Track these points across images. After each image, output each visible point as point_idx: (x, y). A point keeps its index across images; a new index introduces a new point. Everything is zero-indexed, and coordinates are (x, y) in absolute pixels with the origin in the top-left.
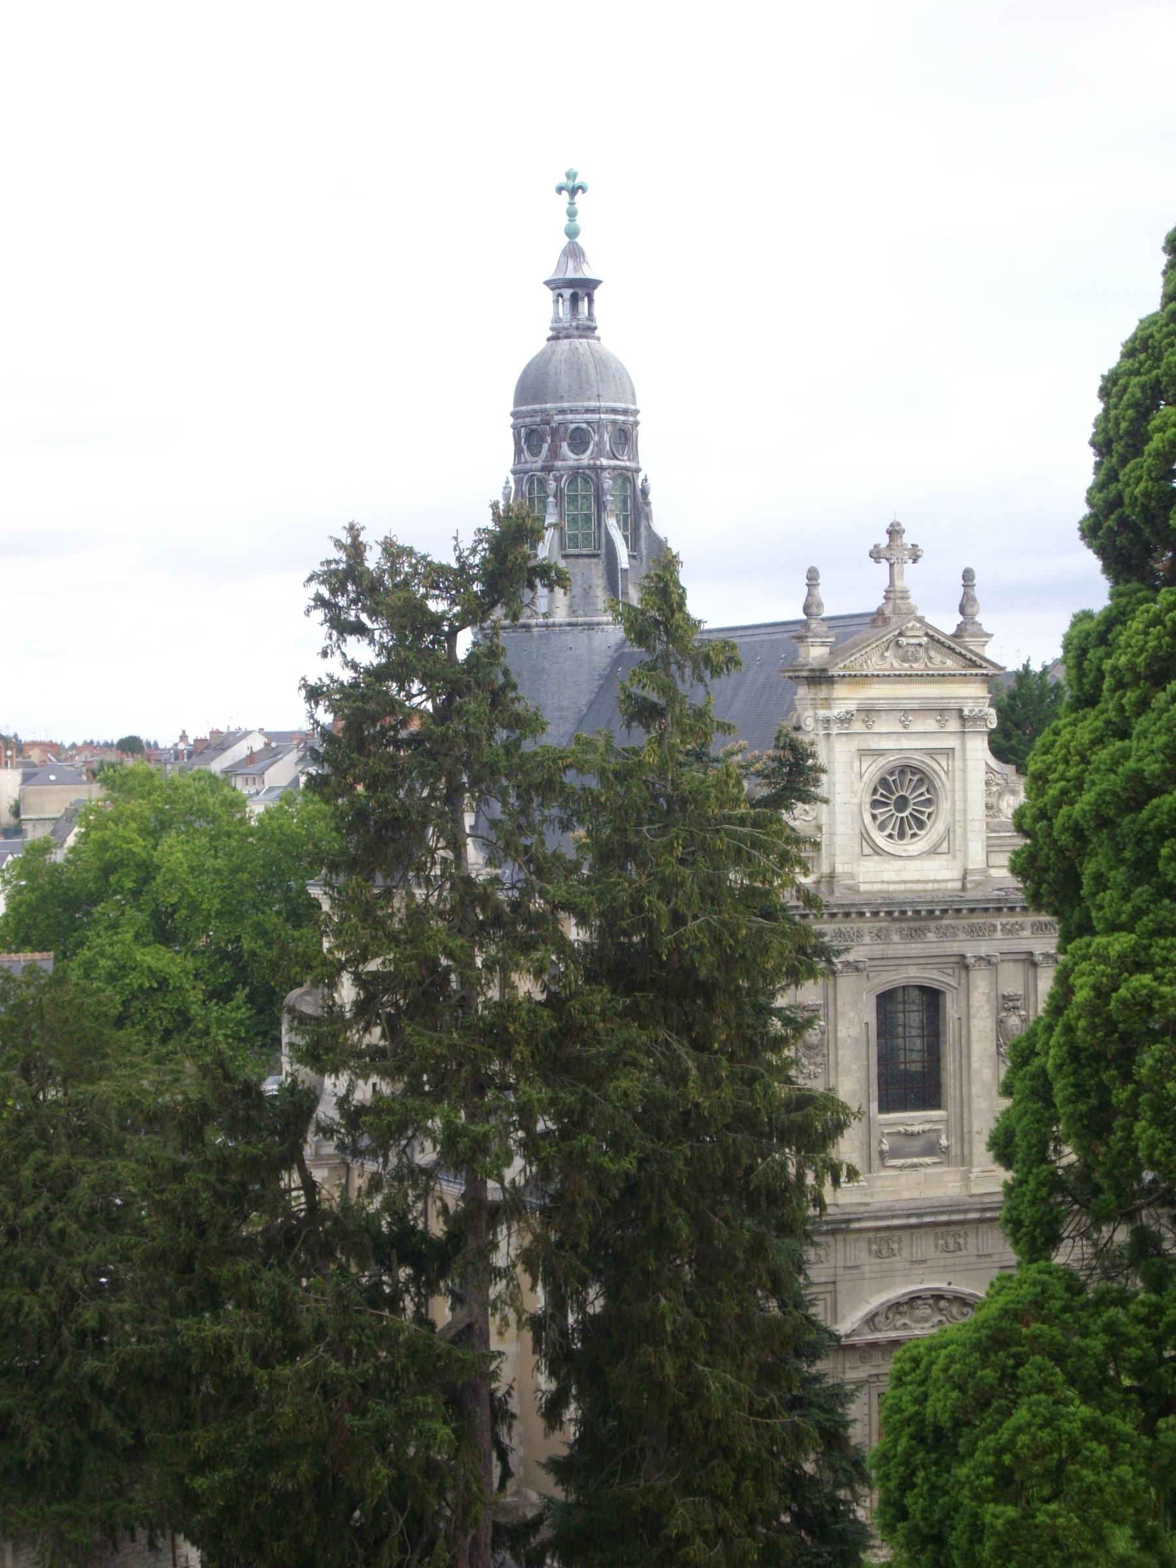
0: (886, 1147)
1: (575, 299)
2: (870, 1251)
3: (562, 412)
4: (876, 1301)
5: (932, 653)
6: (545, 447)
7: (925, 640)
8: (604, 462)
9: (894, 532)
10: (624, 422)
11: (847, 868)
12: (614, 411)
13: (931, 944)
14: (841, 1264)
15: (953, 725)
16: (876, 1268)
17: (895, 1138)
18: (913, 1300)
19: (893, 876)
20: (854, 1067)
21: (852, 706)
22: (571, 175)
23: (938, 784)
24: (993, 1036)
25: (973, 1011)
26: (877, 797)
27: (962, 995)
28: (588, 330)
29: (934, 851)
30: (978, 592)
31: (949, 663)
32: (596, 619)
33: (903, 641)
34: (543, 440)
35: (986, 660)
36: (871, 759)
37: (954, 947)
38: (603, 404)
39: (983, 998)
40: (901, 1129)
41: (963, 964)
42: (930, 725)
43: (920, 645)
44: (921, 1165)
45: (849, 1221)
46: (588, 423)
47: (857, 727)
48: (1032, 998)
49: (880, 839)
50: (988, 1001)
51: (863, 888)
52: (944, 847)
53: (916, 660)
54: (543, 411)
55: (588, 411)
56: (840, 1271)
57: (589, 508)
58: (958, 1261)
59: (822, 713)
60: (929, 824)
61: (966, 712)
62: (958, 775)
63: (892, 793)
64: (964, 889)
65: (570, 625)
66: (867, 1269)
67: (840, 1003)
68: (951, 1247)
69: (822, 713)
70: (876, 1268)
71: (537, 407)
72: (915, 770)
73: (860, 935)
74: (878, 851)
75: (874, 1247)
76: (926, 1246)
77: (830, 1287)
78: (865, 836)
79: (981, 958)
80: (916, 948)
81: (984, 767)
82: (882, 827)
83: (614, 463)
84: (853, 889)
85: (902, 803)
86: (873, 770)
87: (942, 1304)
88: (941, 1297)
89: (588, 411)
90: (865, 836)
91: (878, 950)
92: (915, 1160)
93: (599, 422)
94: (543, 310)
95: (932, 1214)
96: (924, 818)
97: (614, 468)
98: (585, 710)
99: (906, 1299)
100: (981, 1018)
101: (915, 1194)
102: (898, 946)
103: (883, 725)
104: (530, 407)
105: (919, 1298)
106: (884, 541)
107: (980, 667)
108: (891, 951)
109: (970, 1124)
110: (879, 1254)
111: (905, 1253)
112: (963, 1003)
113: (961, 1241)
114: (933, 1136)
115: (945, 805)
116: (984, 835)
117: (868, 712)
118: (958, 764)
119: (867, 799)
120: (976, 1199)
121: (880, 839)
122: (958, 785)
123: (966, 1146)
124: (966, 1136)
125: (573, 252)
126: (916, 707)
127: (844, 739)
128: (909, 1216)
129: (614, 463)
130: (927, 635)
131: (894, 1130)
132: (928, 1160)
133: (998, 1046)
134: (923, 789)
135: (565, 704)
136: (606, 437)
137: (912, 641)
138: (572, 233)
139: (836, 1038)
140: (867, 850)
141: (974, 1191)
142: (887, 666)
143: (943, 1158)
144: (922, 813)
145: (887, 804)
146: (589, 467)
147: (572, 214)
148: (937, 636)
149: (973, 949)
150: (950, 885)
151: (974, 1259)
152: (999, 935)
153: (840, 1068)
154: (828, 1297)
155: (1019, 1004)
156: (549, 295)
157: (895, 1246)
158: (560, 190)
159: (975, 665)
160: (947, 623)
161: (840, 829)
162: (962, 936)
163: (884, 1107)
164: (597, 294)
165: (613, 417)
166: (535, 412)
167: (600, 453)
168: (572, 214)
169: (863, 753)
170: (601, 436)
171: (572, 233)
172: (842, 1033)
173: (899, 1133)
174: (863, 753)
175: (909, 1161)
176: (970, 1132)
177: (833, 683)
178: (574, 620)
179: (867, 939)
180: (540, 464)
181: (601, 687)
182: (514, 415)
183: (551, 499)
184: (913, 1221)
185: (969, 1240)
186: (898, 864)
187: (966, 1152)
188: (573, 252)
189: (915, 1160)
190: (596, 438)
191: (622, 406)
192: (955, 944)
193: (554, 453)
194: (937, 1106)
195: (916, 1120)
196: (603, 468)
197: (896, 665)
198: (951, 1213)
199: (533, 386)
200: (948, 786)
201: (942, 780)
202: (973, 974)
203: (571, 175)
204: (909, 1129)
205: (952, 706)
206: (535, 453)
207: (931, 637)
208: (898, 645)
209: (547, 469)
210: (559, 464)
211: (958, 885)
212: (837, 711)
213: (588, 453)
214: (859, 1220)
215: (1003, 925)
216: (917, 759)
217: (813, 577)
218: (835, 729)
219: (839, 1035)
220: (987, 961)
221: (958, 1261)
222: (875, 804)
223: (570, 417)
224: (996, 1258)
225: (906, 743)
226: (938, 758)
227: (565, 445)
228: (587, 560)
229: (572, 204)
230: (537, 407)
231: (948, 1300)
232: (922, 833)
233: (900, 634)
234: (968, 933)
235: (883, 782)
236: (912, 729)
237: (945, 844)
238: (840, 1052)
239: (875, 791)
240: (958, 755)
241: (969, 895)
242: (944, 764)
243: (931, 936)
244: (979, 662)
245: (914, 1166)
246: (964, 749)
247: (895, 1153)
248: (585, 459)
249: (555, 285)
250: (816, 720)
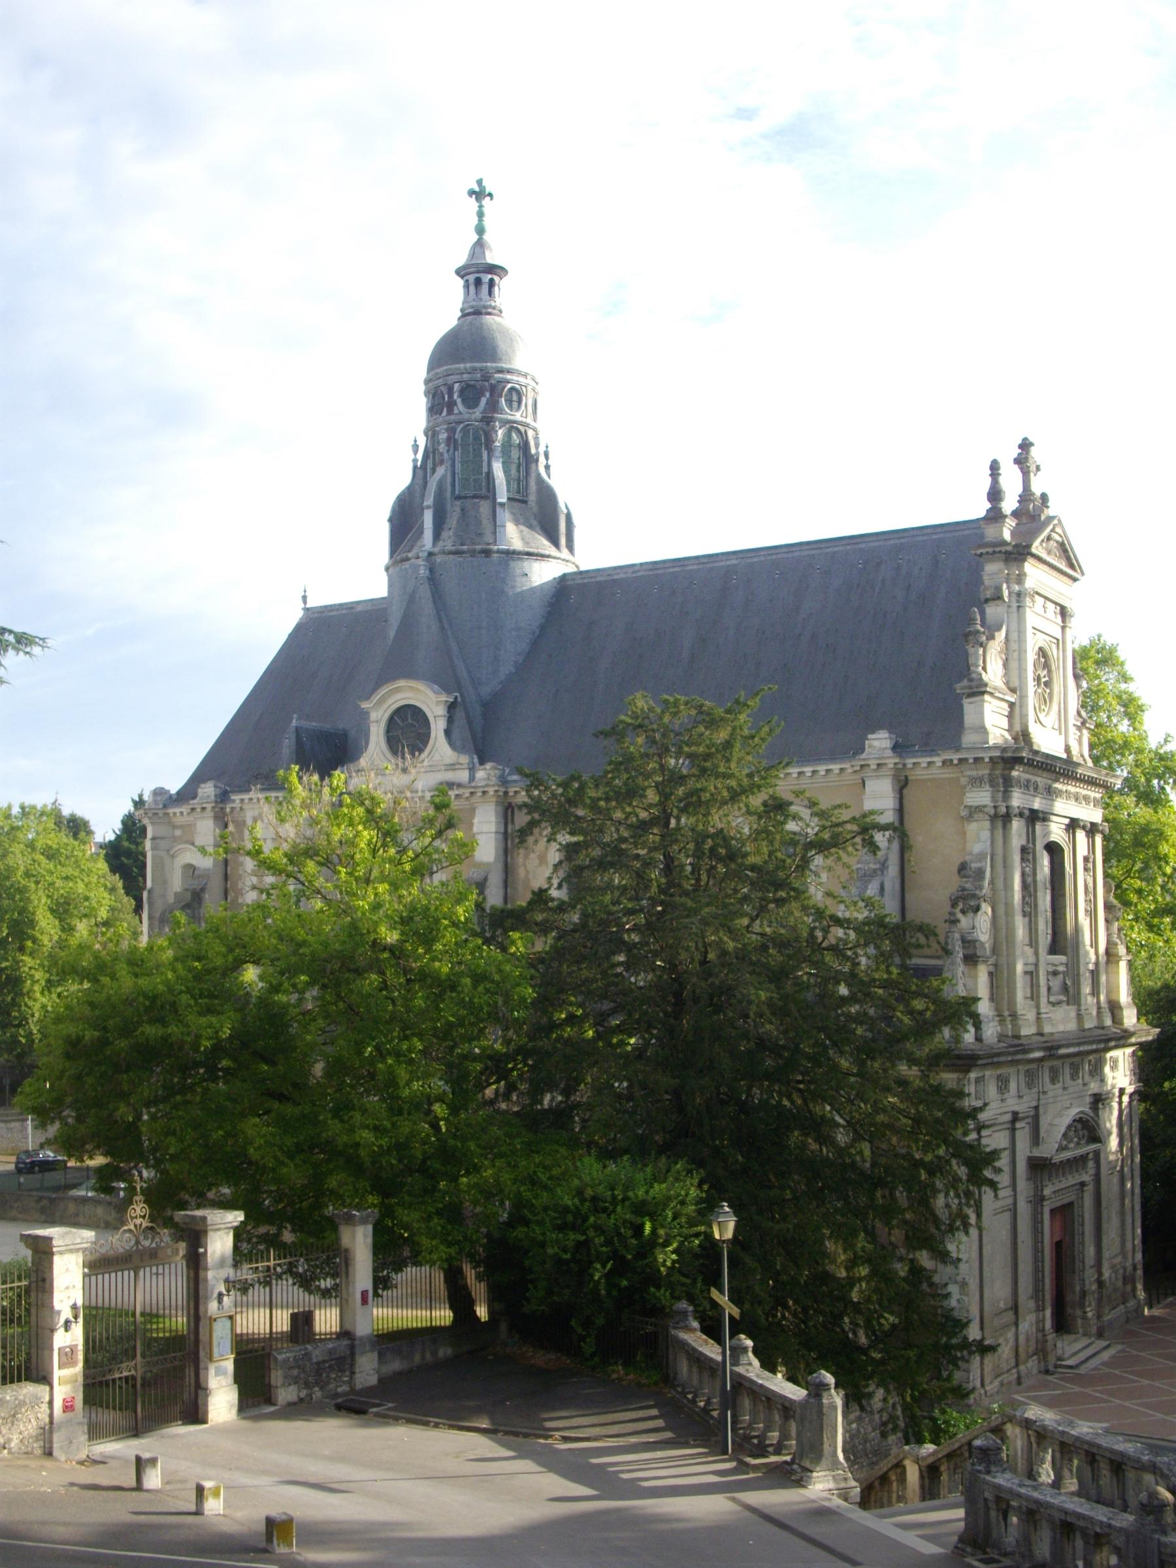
6: (484, 400)
23: (1053, 668)
32: (547, 553)
34: (483, 395)
41: (1073, 825)
98: (537, 631)
104: (468, 365)
120: (1087, 1034)
138: (480, 230)
147: (481, 215)
158: (472, 193)
166: (474, 369)
168: (481, 215)
171: (480, 230)
181: (549, 613)
198: (1079, 1044)
217: (994, 468)
223: (509, 377)
229: (481, 207)
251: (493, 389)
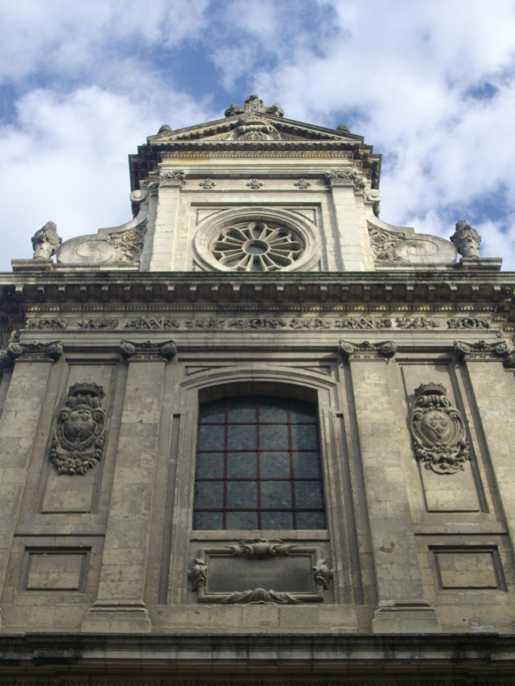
17: (226, 562)
20: (144, 456)
23: (301, 228)
24: (405, 435)
27: (343, 391)
36: (210, 212)
37: (325, 339)
40: (237, 547)
42: (289, 185)
43: (265, 131)
44: (274, 599)
63: (245, 240)
72: (275, 223)
91: (199, 339)
96: (290, 257)
100: (376, 410)
102: (230, 332)
107: (340, 139)
123: (365, 573)
124: (365, 559)
127: (171, 191)
130: (271, 123)
131: (221, 547)
132: (292, 596)
133: (415, 447)
137: (252, 126)
139: (119, 425)
143: (321, 592)
153: (120, 457)
172: (129, 417)
173: (232, 554)
176: (371, 553)
187: (366, 580)
192: (323, 335)
200: (316, 230)
202: (354, 366)
205: (311, 171)
219: (124, 420)
222: (220, 247)
236: (262, 188)
238: (123, 439)
239: (221, 238)
240: (325, 207)
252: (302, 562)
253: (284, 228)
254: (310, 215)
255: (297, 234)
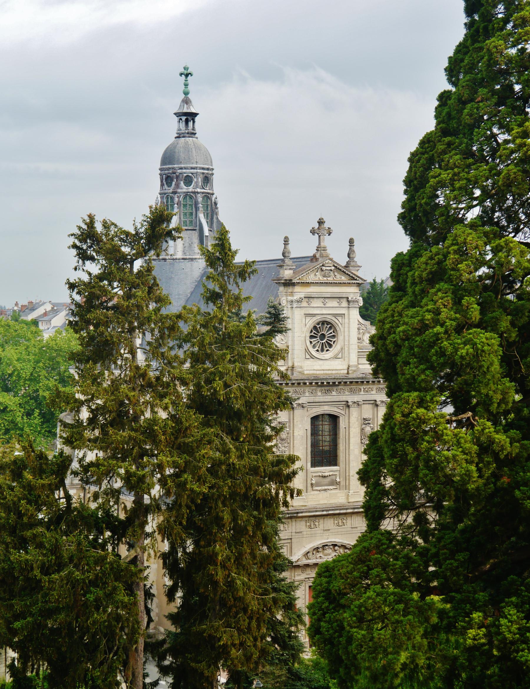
0: (314, 482)
1: (187, 121)
2: (306, 526)
3: (181, 168)
4: (309, 547)
5: (336, 274)
6: (174, 183)
7: (333, 268)
8: (199, 190)
9: (321, 222)
10: (207, 174)
11: (299, 364)
12: (203, 169)
13: (334, 396)
14: (294, 531)
15: (345, 304)
16: (308, 533)
18: (324, 546)
19: (318, 368)
21: (302, 296)
22: (186, 68)
23: (338, 329)
25: (351, 425)
26: (312, 334)
27: (347, 418)
28: (193, 134)
29: (336, 357)
30: (355, 248)
31: (343, 278)
32: (194, 257)
33: (324, 268)
34: (172, 180)
35: (359, 277)
37: (344, 398)
38: (198, 166)
39: (356, 419)
40: (320, 474)
42: (334, 303)
45: (298, 513)
46: (192, 174)
47: (304, 304)
48: (376, 419)
49: (313, 352)
50: (357, 421)
51: (306, 372)
52: (340, 356)
53: (329, 277)
54: (173, 168)
55: (192, 168)
56: (294, 534)
57: (192, 209)
58: (343, 530)
59: (290, 298)
60: (334, 345)
61: (350, 299)
62: (346, 325)
63: (318, 332)
64: (348, 373)
65: (183, 259)
66: (305, 533)
67: (295, 421)
68: (340, 524)
69: (290, 298)
70: (308, 533)
71: (170, 166)
72: (328, 323)
73: (304, 393)
74: (312, 357)
75: (308, 524)
76: (330, 523)
77: (289, 541)
78: (307, 351)
79: (355, 402)
80: (328, 398)
81: (357, 323)
82: (314, 347)
83: (203, 190)
84: (301, 373)
85: (323, 336)
86: (311, 322)
87: (336, 548)
88: (336, 545)
89: (192, 168)
90: (307, 351)
91: (312, 399)
92: (326, 487)
93: (196, 173)
94: (174, 125)
95: (333, 510)
96: (332, 343)
97: (203, 193)
98: (189, 295)
99: (321, 546)
101: (326, 502)
102: (320, 396)
103: (316, 303)
105: (327, 545)
106: (316, 226)
108: (317, 399)
109: (349, 472)
110: (310, 527)
111: (321, 526)
112: (347, 421)
113: (345, 521)
114: (334, 477)
115: (340, 338)
116: (357, 351)
117: (309, 298)
118: (346, 320)
119: (308, 335)
120: (351, 504)
121: (313, 352)
122: (346, 329)
125: (186, 101)
126: (329, 296)
127: (299, 309)
128: (323, 511)
129: (203, 190)
130: (334, 266)
133: (361, 440)
134: (332, 331)
135: (181, 292)
136: (200, 180)
138: (186, 93)
140: (308, 357)
141: (351, 500)
142: (317, 279)
144: (331, 341)
145: (316, 337)
146: (192, 192)
147: (186, 85)
148: (338, 267)
149: (351, 398)
150: (342, 372)
151: (350, 529)
152: (362, 393)
154: (288, 545)
155: (370, 422)
156: (176, 119)
157: (317, 524)
158: (181, 74)
159: (354, 279)
160: (342, 261)
161: (296, 347)
162: (347, 393)
163: (313, 465)
164: (197, 119)
165: (202, 171)
166: (170, 168)
167: (197, 187)
168: (186, 85)
169: (307, 315)
170: (198, 179)
171: (186, 93)
173: (319, 476)
174: (307, 315)
175: (324, 488)
176: (349, 476)
177: (294, 285)
178: (185, 257)
179: (307, 394)
180: (171, 191)
181: (196, 286)
182: (161, 169)
183: (176, 205)
184: (325, 513)
185: (348, 521)
186: (321, 362)
188: (186, 101)
189: (326, 487)
190: (195, 180)
191: (207, 166)
193: (178, 186)
194: (336, 465)
195: (326, 470)
196: (198, 193)
197: (321, 278)
198: (340, 510)
199: (168, 158)
200: (342, 330)
201: (340, 328)
203: (186, 68)
204: (324, 474)
205: (344, 296)
206: (169, 185)
207: (336, 267)
208: (322, 270)
209: (175, 193)
210: (179, 190)
211: (346, 372)
212: (296, 297)
213: (192, 186)
214: (302, 512)
215: (364, 389)
216: (329, 318)
217: (286, 241)
218: (295, 305)
220: (357, 404)
221: (343, 530)
222: (311, 337)
223: (184, 171)
224: (359, 529)
225: (325, 311)
226: (338, 318)
227: (182, 183)
228: (191, 232)
230: (170, 166)
231: (339, 546)
232: (331, 349)
233: (323, 265)
234: (349, 392)
235: (315, 328)
236: (327, 305)
237: (340, 354)
239: (311, 331)
240: (346, 316)
241: (350, 376)
242: (340, 320)
243: (334, 393)
244: (355, 278)
245: (325, 490)
246: (349, 314)
247: (318, 485)
248: (191, 189)
249: (177, 114)
250: (287, 301)
251: (177, 177)
252: (334, 477)
253: (331, 326)
254: (340, 319)
255: (335, 331)
